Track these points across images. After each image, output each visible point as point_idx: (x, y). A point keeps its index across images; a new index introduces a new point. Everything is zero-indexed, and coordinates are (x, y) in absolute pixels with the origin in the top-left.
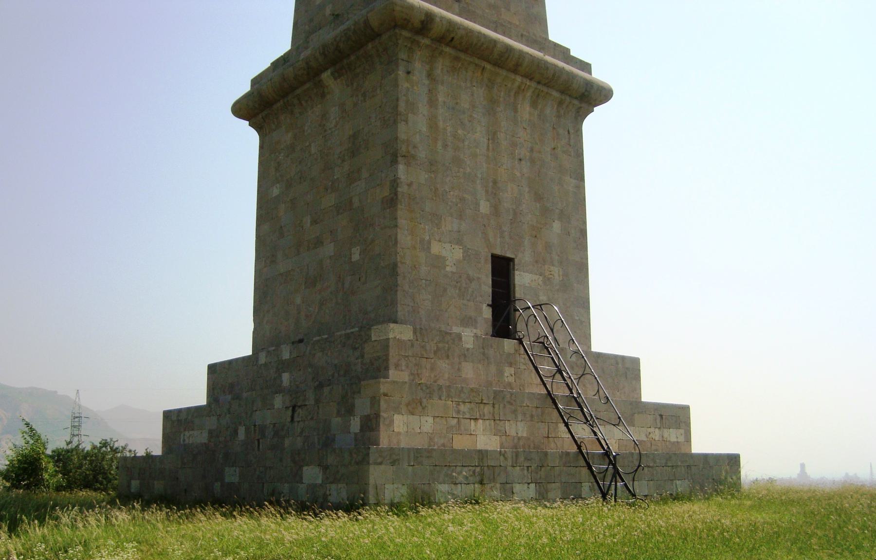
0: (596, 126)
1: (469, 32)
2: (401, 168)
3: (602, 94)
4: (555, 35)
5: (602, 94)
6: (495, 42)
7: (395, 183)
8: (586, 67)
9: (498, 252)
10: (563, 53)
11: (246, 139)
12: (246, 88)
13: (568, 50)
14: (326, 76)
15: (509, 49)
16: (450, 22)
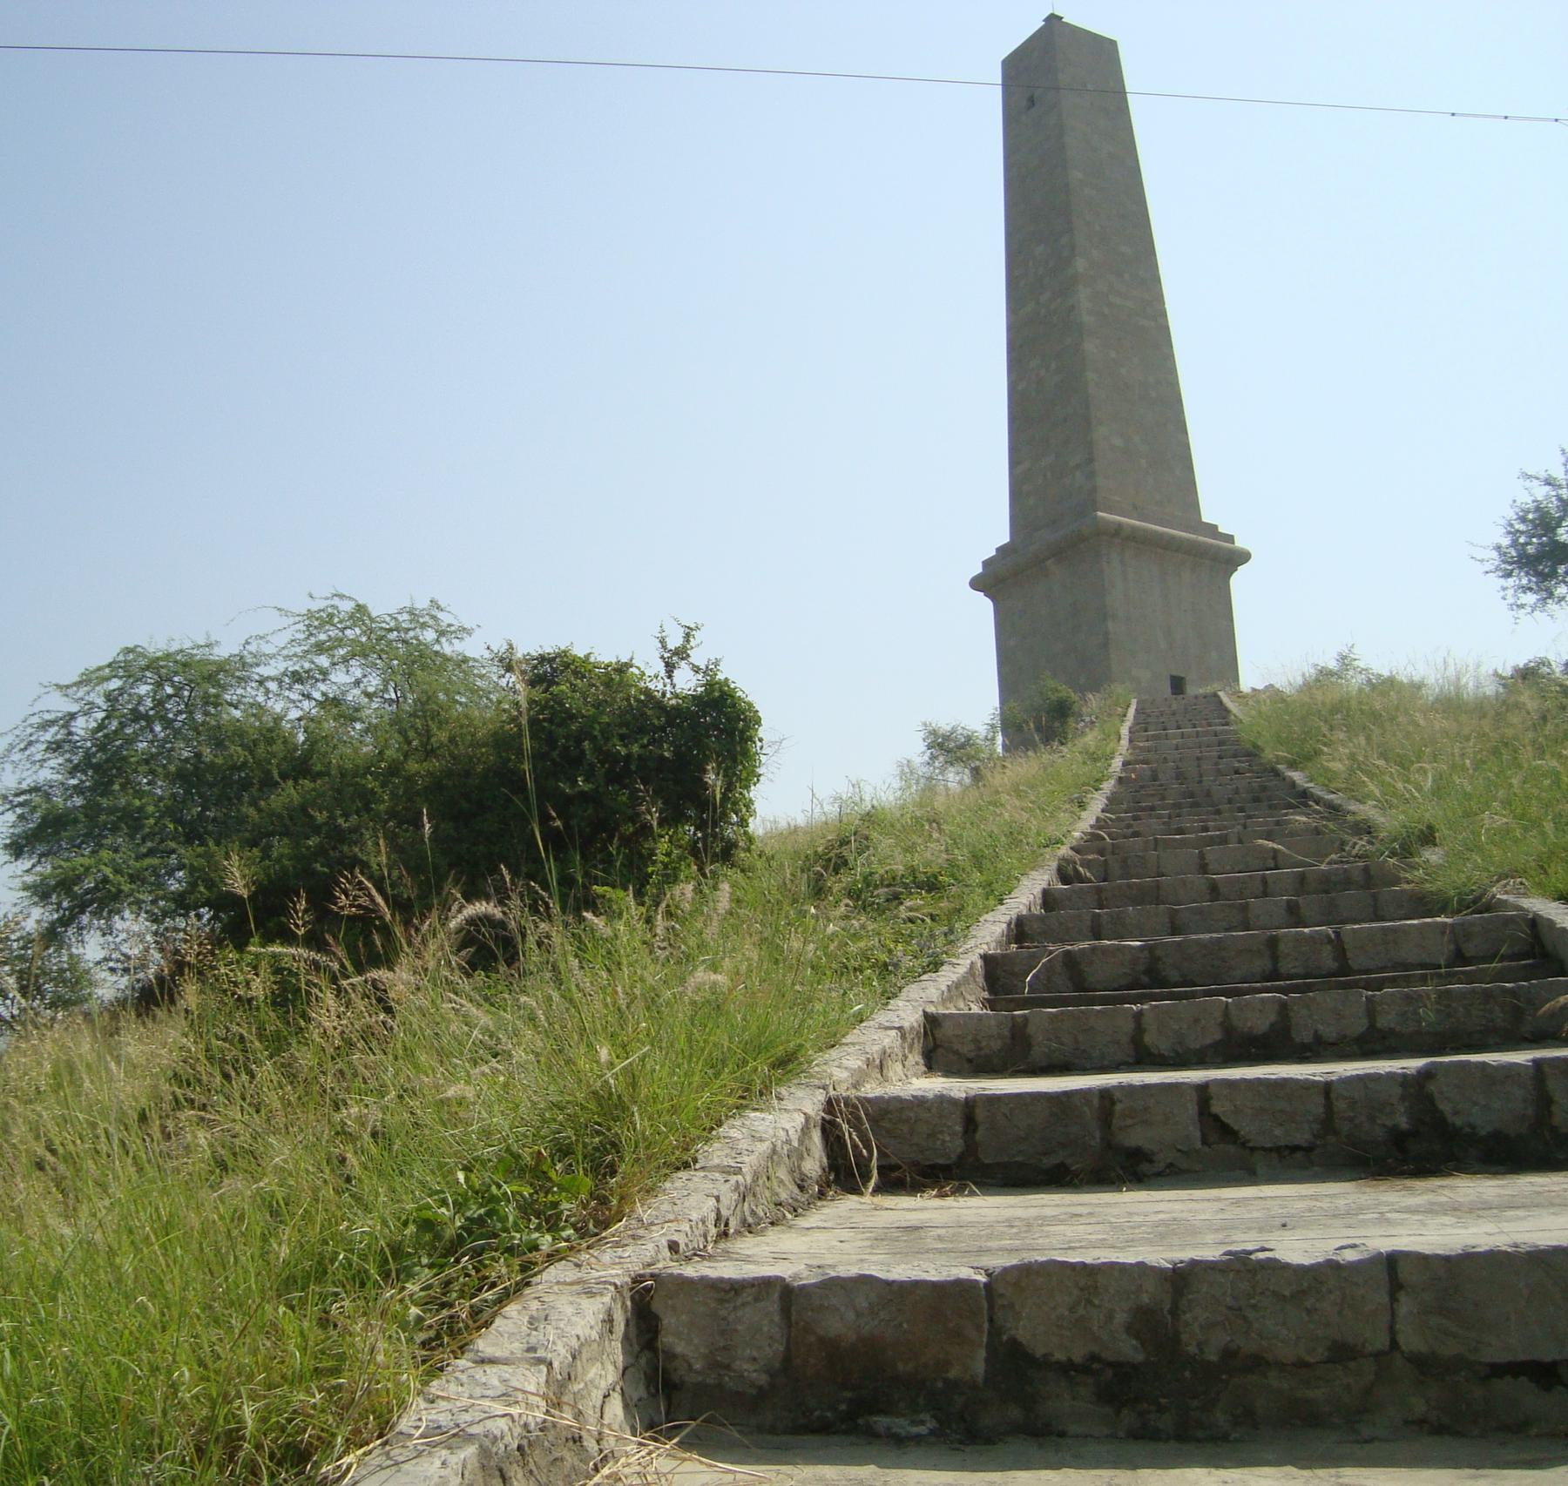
0: (1241, 583)
1: (1145, 530)
2: (1110, 625)
3: (1244, 557)
4: (1206, 517)
5: (1244, 557)
6: (1162, 535)
7: (1106, 633)
8: (1230, 539)
9: (1174, 673)
10: (1212, 530)
11: (983, 607)
12: (979, 570)
13: (1216, 527)
14: (1049, 562)
15: (1173, 538)
16: (1133, 528)
